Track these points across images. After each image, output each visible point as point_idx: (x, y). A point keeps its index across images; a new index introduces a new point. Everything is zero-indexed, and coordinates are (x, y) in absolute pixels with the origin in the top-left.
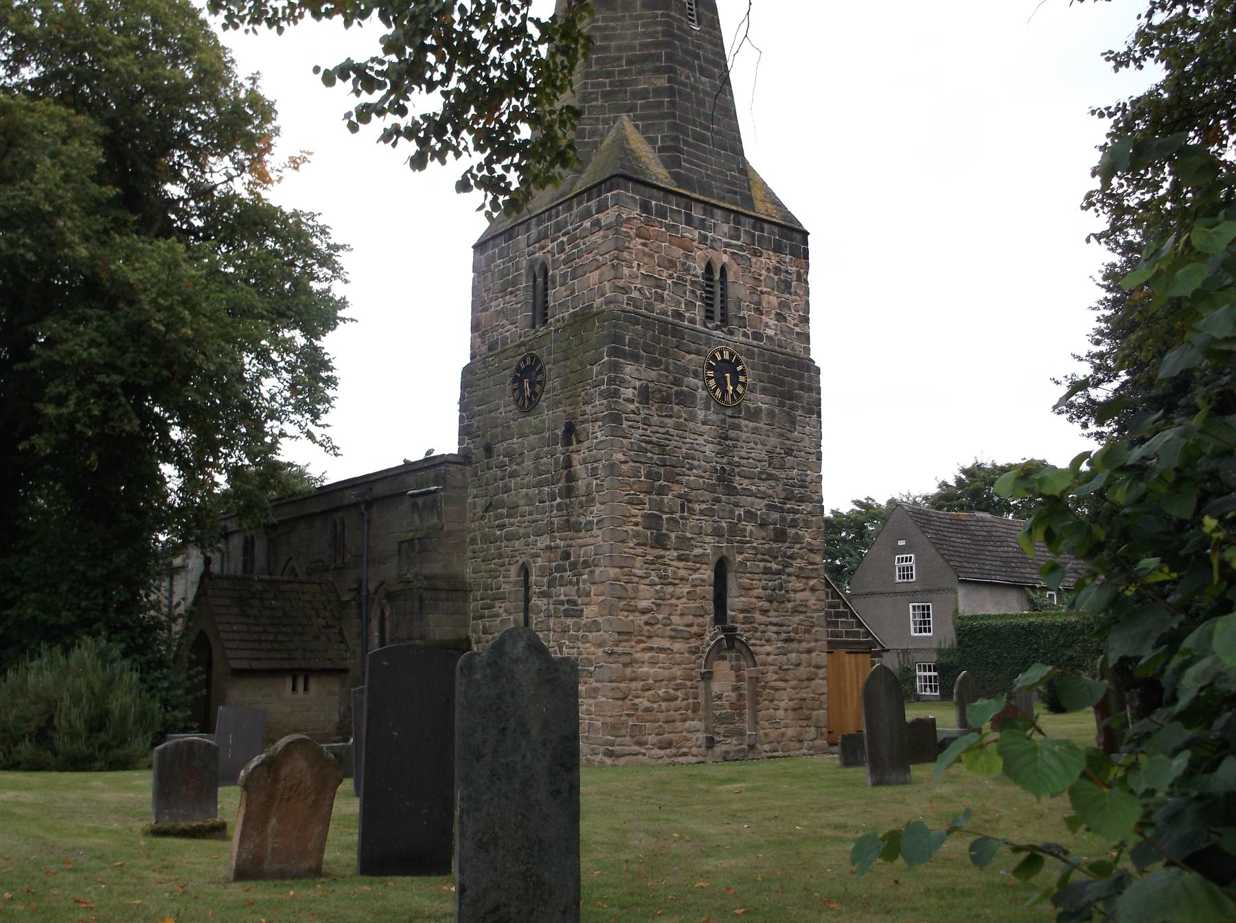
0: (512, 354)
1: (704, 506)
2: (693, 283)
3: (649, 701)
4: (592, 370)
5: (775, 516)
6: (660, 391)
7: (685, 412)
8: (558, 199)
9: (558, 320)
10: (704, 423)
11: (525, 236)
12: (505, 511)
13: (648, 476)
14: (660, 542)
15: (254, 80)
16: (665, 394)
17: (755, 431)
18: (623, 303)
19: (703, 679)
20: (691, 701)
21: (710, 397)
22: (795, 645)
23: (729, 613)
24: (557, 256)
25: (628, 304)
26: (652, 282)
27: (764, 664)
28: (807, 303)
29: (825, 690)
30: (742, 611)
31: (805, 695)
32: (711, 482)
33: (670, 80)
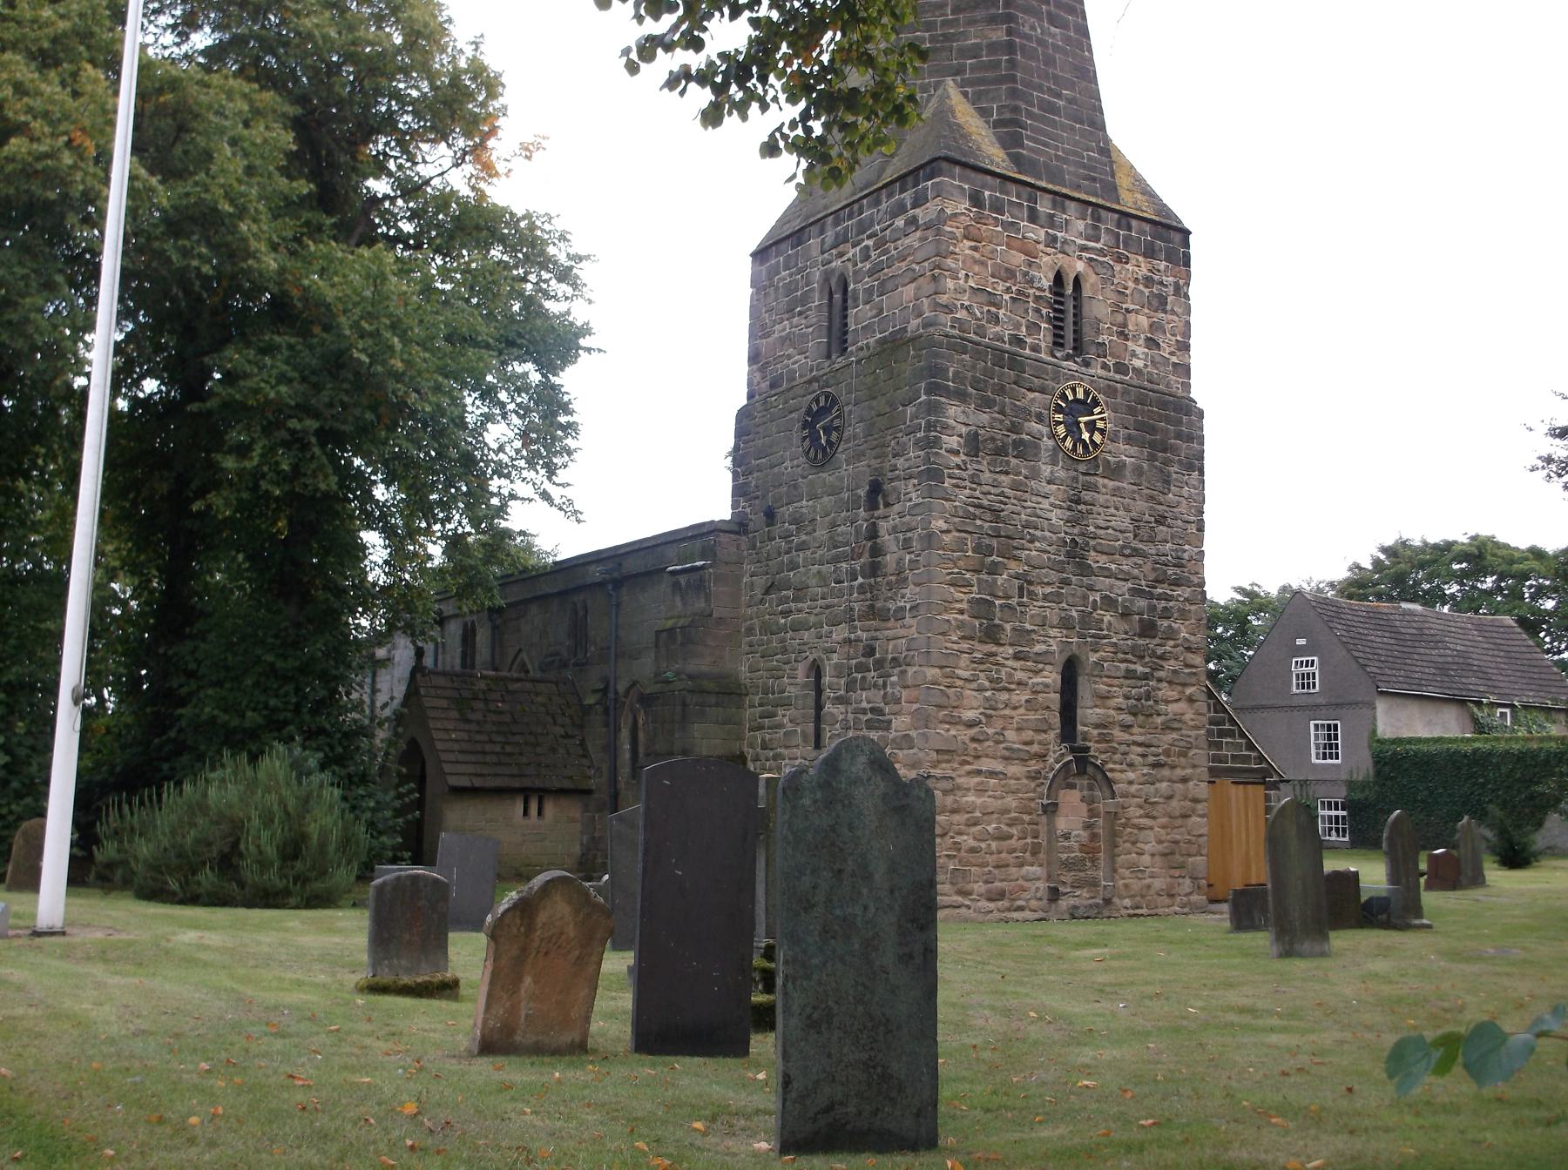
0: (802, 392)
1: (1048, 590)
2: (1037, 299)
3: (975, 838)
4: (904, 412)
5: (1142, 603)
6: (993, 439)
7: (1026, 467)
8: (862, 190)
9: (862, 349)
10: (1049, 482)
11: (819, 240)
12: (790, 593)
13: (978, 549)
14: (991, 634)
15: (476, 45)
16: (999, 444)
17: (1116, 492)
18: (945, 326)
19: (1045, 812)
20: (1029, 840)
21: (1057, 449)
22: (1166, 772)
23: (1080, 728)
24: (860, 265)
25: (953, 327)
26: (983, 298)
27: (1125, 795)
28: (1188, 324)
29: (1204, 831)
30: (1097, 726)
31: (1178, 837)
32: (1058, 558)
33: (1009, 32)
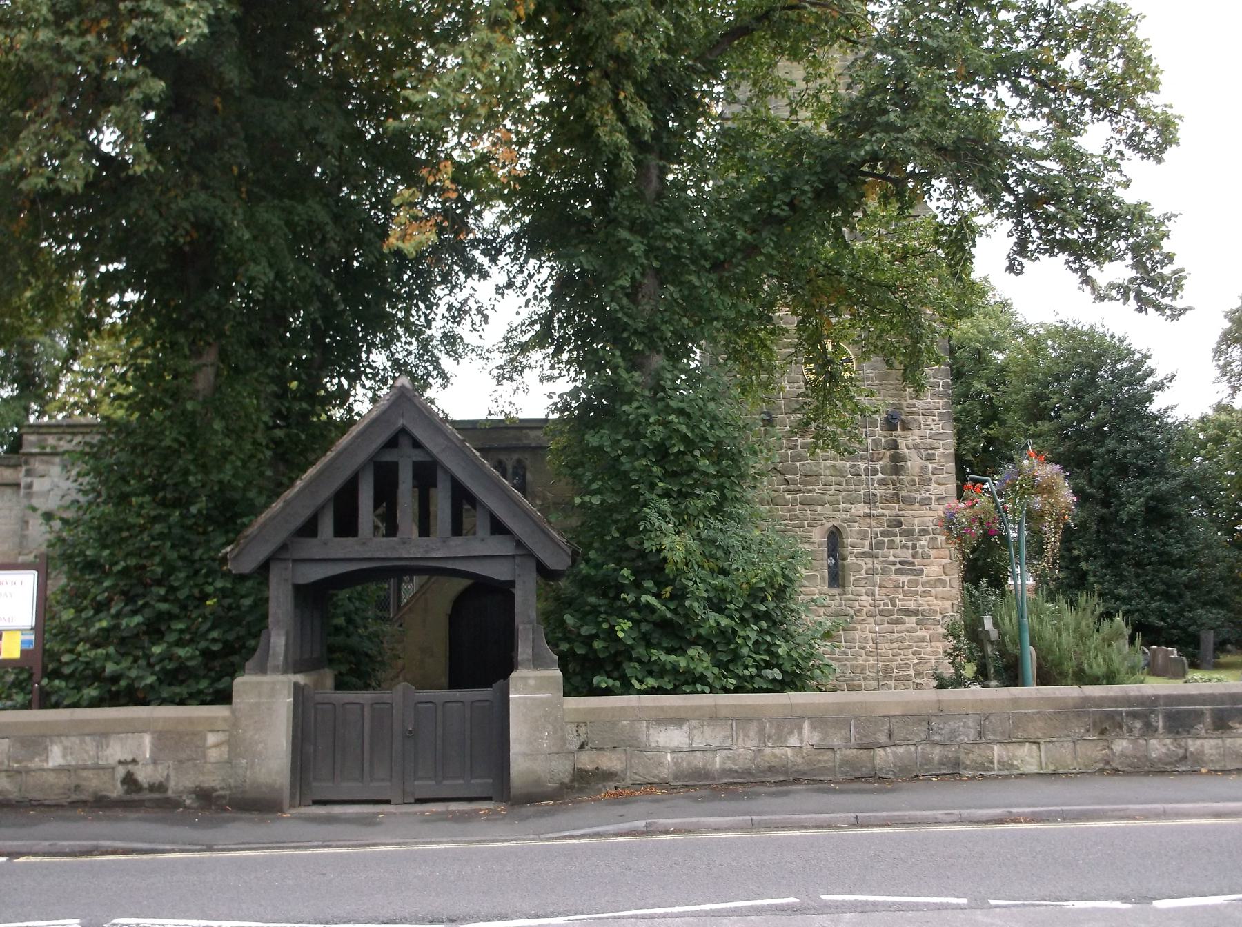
12: (797, 478)
